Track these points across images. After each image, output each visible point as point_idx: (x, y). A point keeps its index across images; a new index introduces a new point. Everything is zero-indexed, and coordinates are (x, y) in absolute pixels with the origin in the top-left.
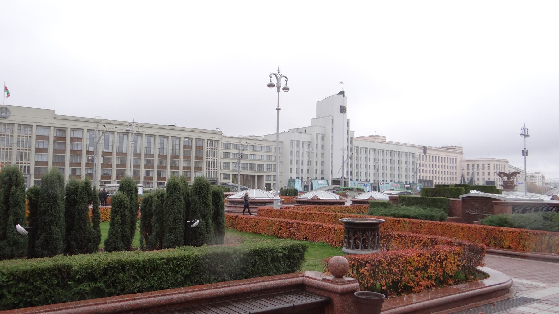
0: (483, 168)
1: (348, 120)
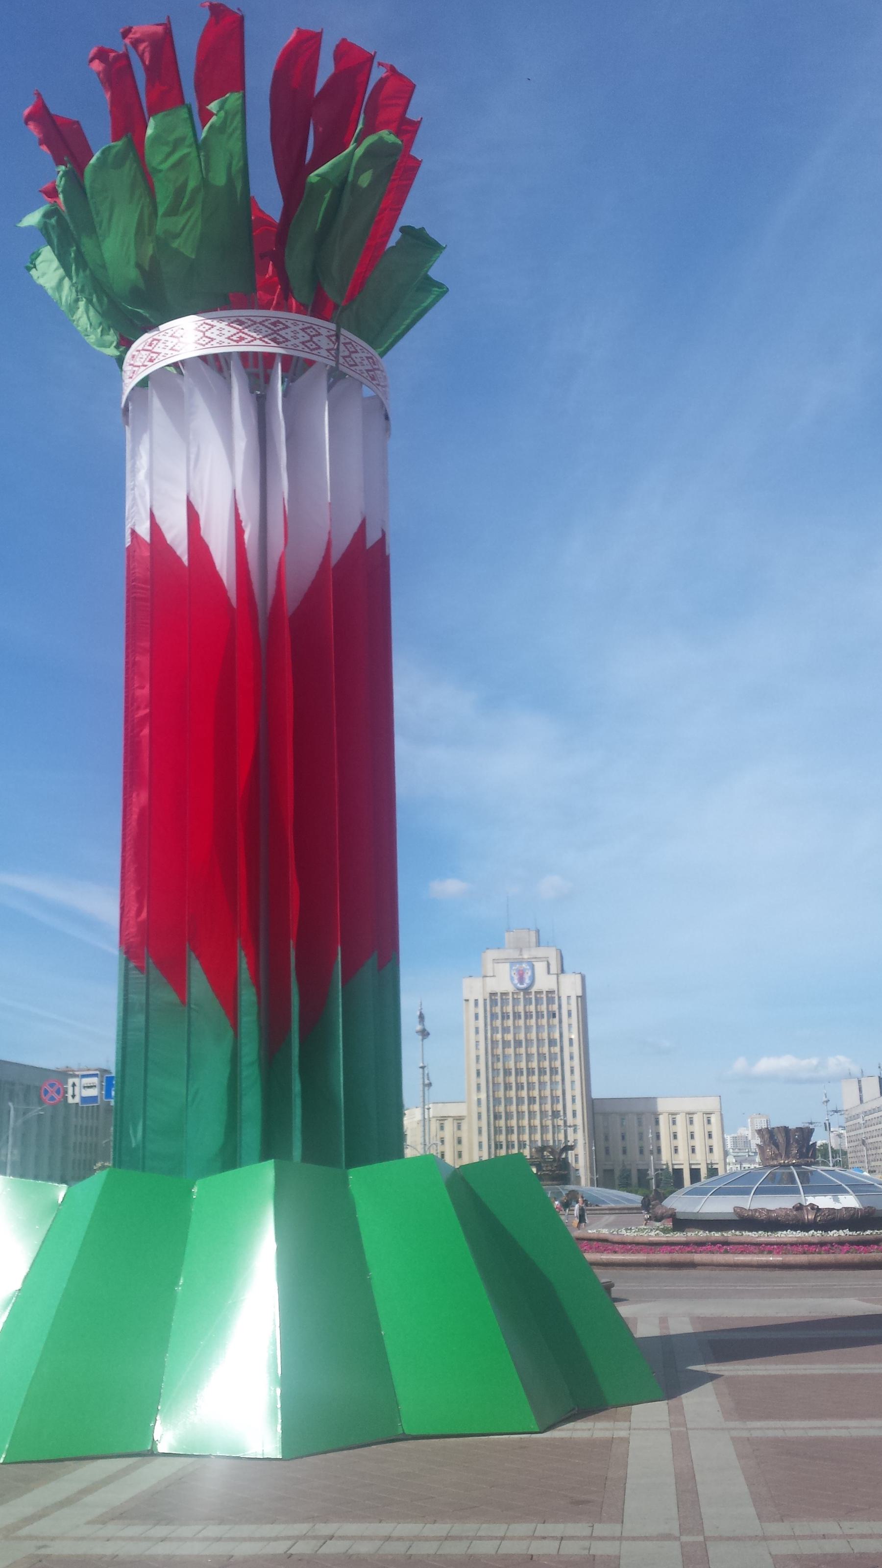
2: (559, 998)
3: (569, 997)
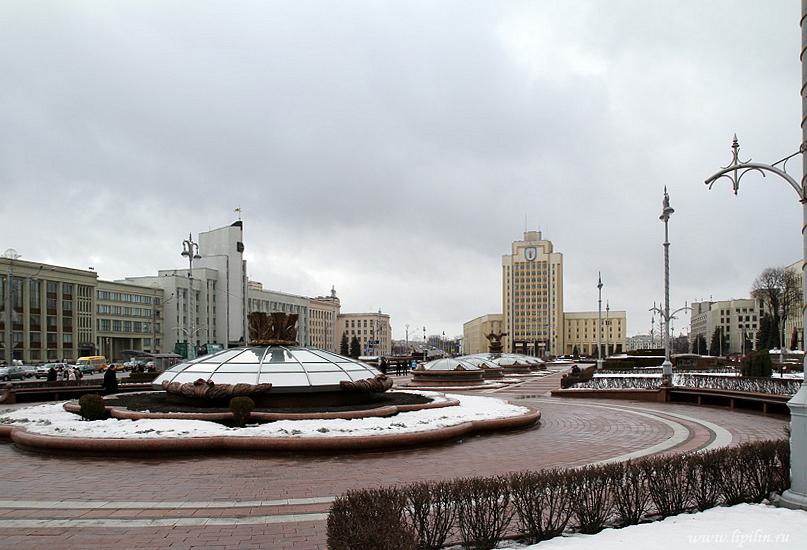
0: (365, 325)
1: (245, 261)
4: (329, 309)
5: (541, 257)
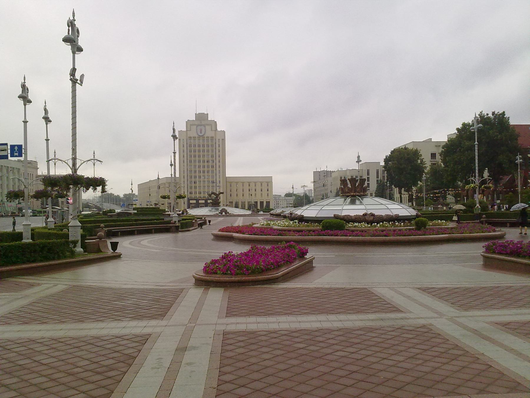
2: (215, 139)
3: (219, 139)
4: (30, 171)
5: (209, 133)
